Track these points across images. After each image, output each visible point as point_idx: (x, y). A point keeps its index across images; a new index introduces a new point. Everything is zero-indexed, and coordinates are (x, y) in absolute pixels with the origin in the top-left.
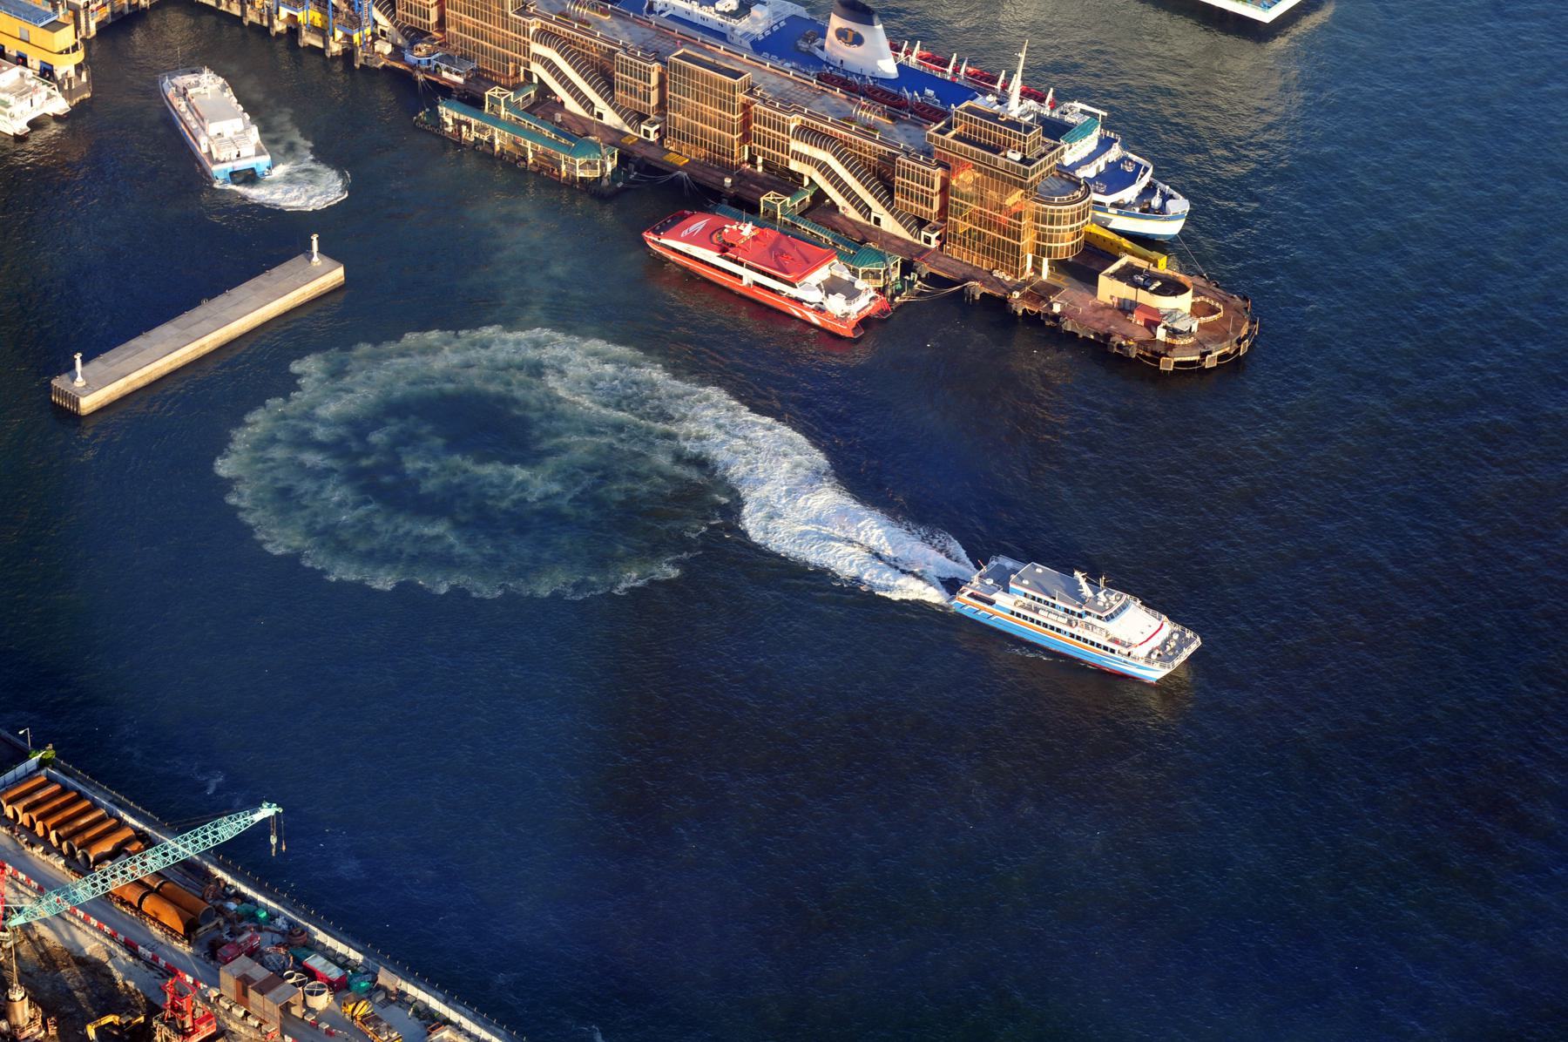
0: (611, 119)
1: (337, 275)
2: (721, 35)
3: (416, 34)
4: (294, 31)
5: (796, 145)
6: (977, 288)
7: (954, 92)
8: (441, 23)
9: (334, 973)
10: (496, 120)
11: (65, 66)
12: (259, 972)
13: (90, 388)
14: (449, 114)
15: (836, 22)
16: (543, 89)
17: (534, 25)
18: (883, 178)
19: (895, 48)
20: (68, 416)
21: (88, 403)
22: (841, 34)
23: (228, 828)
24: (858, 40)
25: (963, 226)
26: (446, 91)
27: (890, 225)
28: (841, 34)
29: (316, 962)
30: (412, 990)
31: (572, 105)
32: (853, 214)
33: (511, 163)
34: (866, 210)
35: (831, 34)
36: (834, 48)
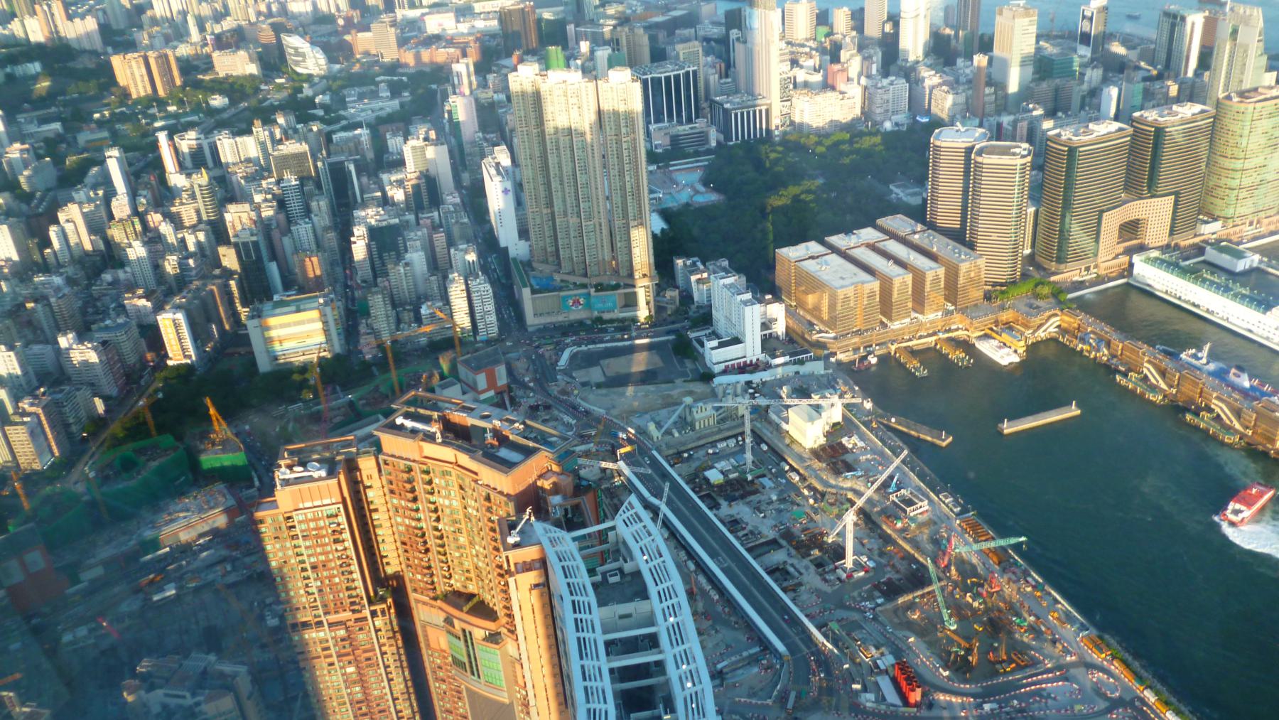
0: (1163, 386)
1: (1078, 412)
2: (1199, 369)
3: (1114, 356)
4: (1082, 350)
5: (1214, 401)
6: (1260, 448)
7: (1264, 394)
8: (1121, 354)
9: (1034, 583)
10: (1131, 381)
11: (1021, 351)
12: (1014, 577)
13: (1007, 428)
14: (1118, 378)
15: (1233, 371)
16: (1146, 376)
17: (1146, 359)
18: (1238, 414)
19: (1250, 380)
20: (1001, 434)
21: (1006, 431)
22: (1234, 374)
23: (1013, 541)
24: (1239, 376)
25: (1259, 431)
26: (1119, 372)
27: (1238, 426)
28: (1234, 374)
29: (1029, 579)
30: (1053, 592)
31: (1153, 381)
32: (1228, 422)
33: (1133, 392)
34: (1231, 422)
35: (1231, 374)
36: (1232, 377)
